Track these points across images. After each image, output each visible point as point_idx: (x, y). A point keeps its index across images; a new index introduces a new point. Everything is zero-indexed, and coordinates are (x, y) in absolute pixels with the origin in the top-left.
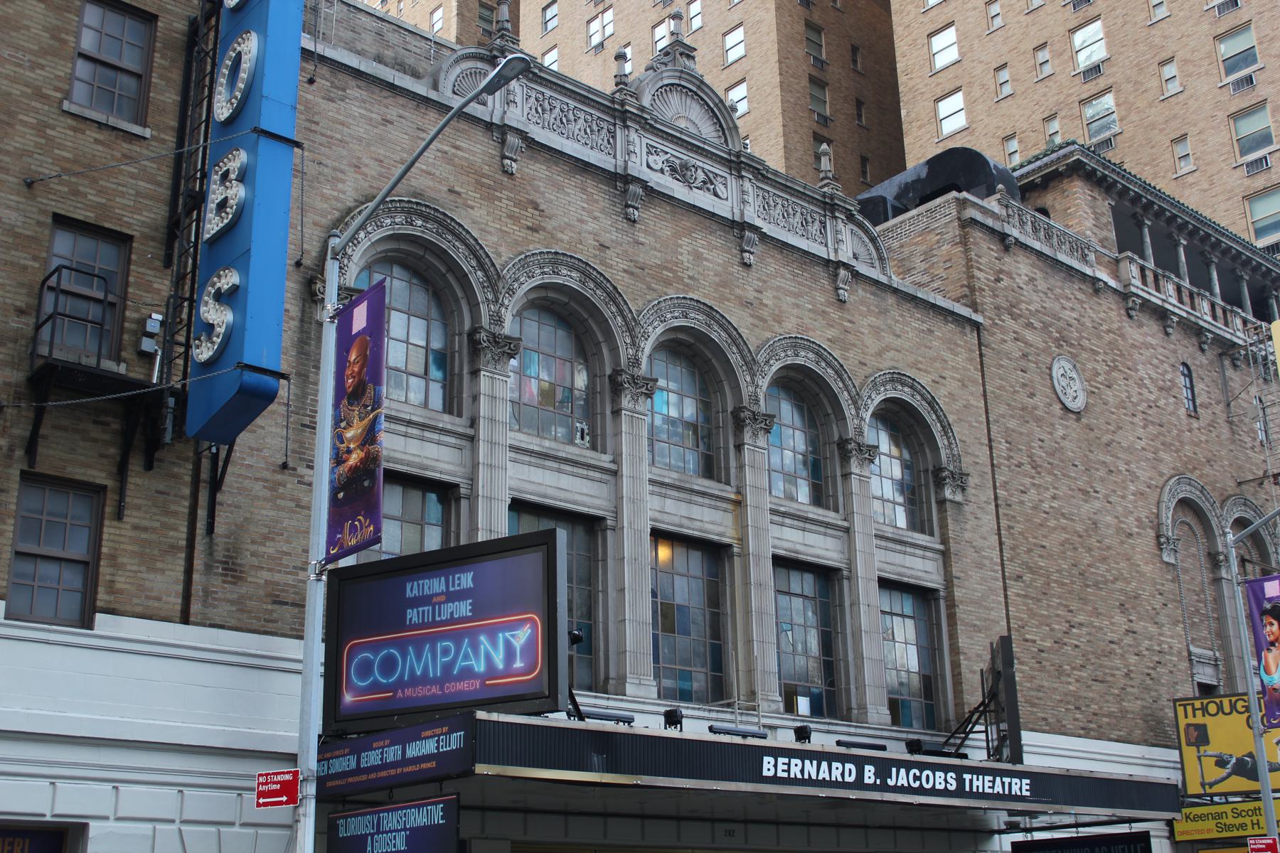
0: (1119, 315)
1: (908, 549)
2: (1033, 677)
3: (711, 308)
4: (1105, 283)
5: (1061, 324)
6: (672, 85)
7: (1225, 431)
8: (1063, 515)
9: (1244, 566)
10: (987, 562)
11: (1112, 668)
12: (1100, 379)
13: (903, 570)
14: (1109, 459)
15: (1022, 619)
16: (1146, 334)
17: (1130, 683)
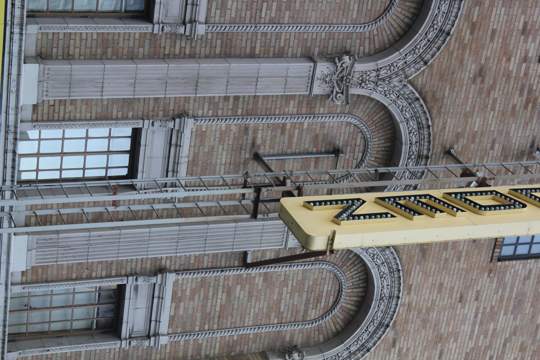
7: (519, 137)
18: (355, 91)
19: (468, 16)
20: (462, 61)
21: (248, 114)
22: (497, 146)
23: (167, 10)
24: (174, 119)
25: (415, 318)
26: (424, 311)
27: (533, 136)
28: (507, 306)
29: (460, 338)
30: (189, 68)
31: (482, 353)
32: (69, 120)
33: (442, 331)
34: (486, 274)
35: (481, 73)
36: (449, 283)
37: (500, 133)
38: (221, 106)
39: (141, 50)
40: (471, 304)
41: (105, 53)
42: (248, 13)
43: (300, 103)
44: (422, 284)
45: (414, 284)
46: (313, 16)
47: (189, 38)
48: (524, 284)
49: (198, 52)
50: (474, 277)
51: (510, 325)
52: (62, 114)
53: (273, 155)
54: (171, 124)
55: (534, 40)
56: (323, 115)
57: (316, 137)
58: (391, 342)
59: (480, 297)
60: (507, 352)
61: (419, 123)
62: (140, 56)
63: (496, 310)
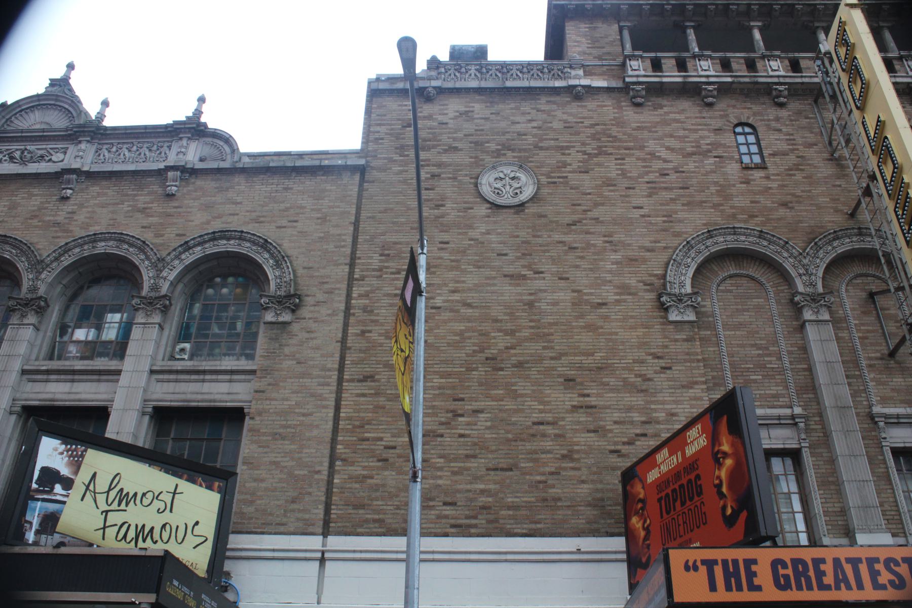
0: (620, 108)
1: (208, 377)
2: (366, 477)
3: (5, 236)
4: (589, 87)
5: (508, 136)
6: (33, 107)
7: (825, 170)
8: (469, 305)
9: (874, 302)
10: (316, 372)
11: (535, 452)
12: (569, 168)
13: (194, 397)
14: (568, 238)
15: (363, 418)
16: (667, 113)
17: (571, 465)
18: (820, 289)
19: (745, 221)
20: (779, 219)
21: (857, 365)
22: (837, 183)
23: (788, 438)
24: (876, 423)
30: (832, 416)
32: (897, 506)
35: (785, 205)
37: (826, 183)
38: (856, 388)
39: (824, 455)
41: (833, 483)
42: (777, 377)
43: (839, 329)
46: (769, 330)
47: (806, 418)
49: (816, 411)
52: (893, 513)
53: (887, 342)
54: (882, 424)
55: (752, 175)
56: (844, 310)
57: (864, 313)
61: (834, 239)
62: (829, 455)
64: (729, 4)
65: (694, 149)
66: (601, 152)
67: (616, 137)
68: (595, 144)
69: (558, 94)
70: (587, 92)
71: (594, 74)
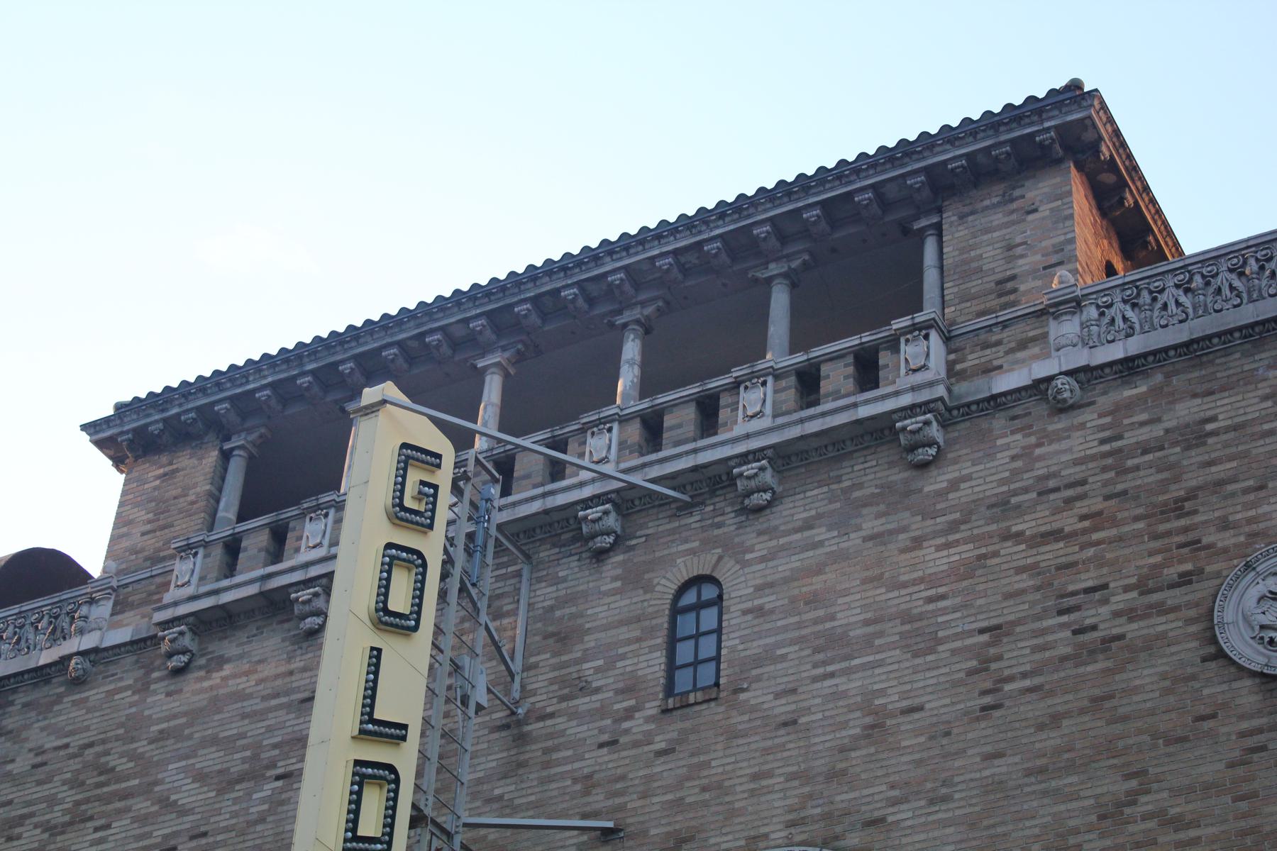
4: (96, 650)
25: (821, 802)
26: (807, 789)
27: (491, 732)
28: (816, 622)
29: (876, 687)
31: (917, 625)
33: (858, 731)
34: (743, 696)
36: (752, 762)
40: (803, 697)
44: (749, 818)
45: (746, 834)
48: (772, 611)
50: (746, 718)
51: (858, 596)
58: (872, 829)
59: (790, 686)
60: (920, 573)
63: (822, 641)
64: (422, 335)
65: (246, 766)
66: (78, 818)
67: (113, 769)
68: (69, 796)
69: (47, 682)
70: (94, 663)
71: (132, 606)
